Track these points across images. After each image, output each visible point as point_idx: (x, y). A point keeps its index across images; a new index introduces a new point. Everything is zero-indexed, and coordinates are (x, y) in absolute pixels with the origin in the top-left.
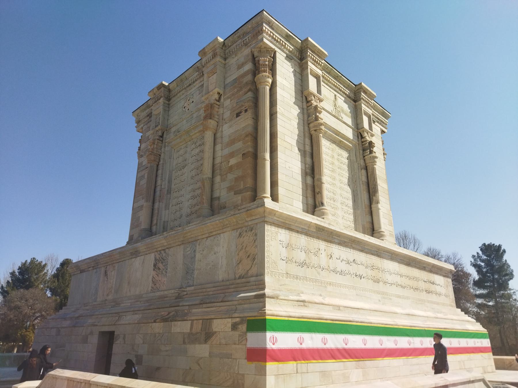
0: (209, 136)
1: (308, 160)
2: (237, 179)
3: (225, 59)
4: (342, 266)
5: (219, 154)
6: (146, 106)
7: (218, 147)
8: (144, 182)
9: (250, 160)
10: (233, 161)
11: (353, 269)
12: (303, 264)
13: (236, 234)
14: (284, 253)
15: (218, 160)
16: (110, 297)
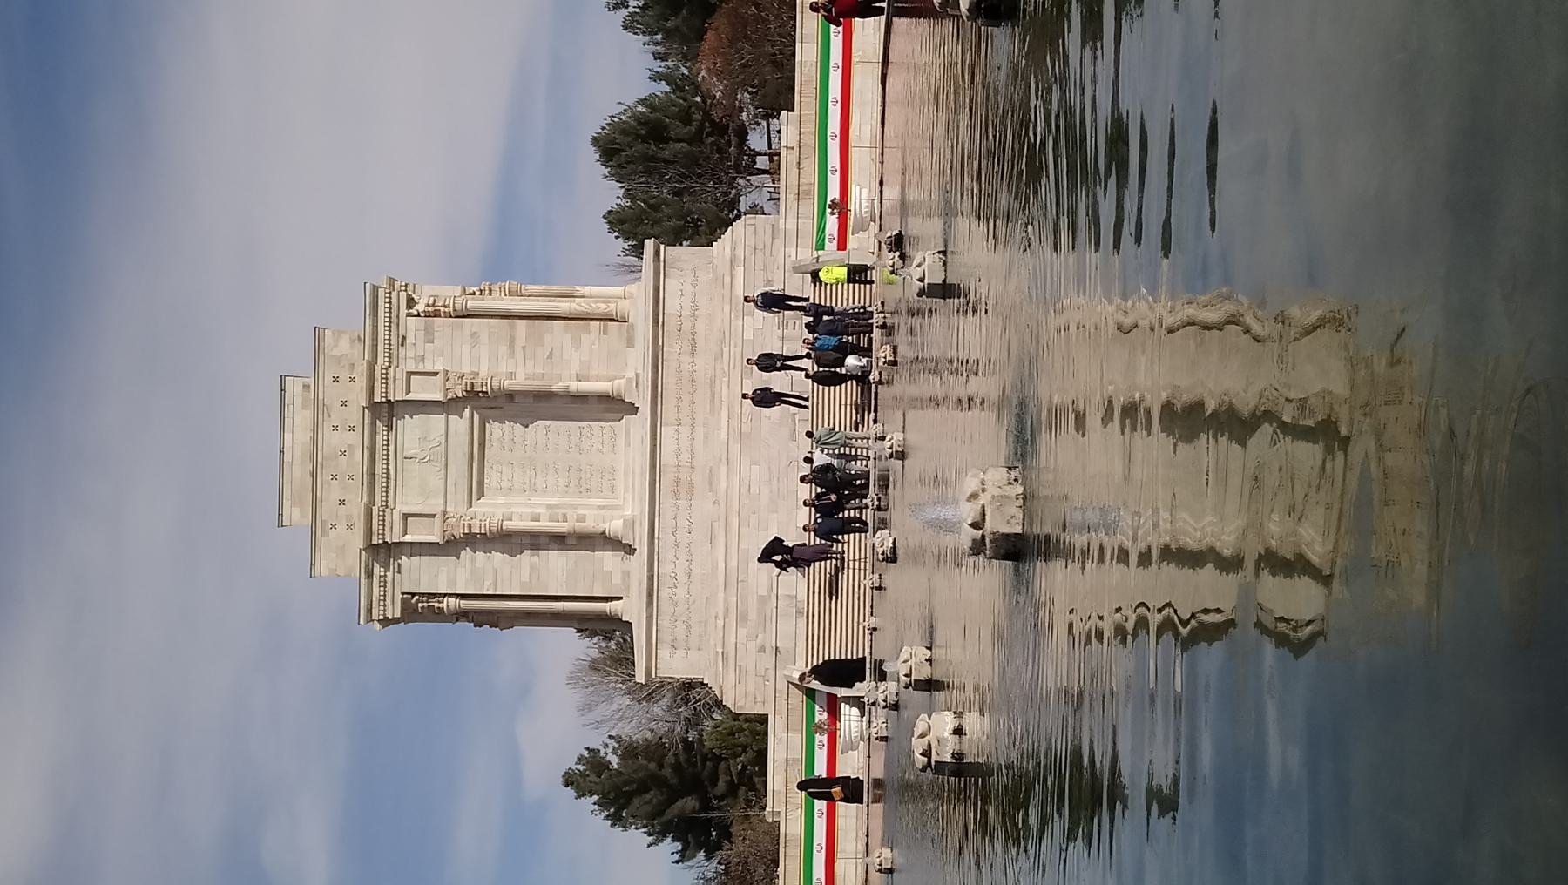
11: (683, 537)
12: (689, 627)
14: (680, 653)
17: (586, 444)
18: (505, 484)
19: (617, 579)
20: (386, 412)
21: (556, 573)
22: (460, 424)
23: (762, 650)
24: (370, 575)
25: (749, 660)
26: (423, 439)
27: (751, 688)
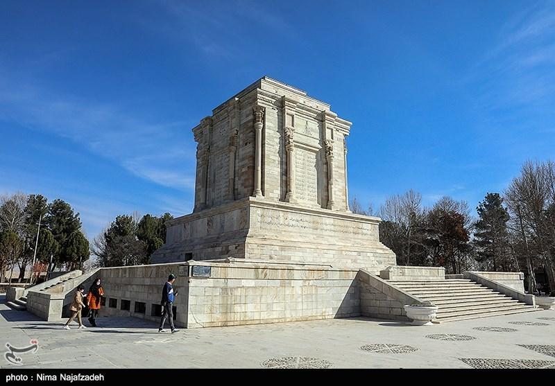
0: (232, 154)
1: (284, 166)
2: (245, 180)
3: (240, 109)
4: (292, 223)
5: (237, 165)
6: (199, 127)
7: (237, 161)
8: (200, 174)
9: (251, 170)
10: (244, 170)
11: (301, 224)
12: (269, 223)
13: (240, 211)
14: (259, 219)
15: (237, 169)
16: (188, 238)
17: (311, 189)
18: (298, 157)
19: (271, 195)
20: (321, 118)
21: (272, 170)
22: (316, 143)
23: (271, 258)
24: (273, 97)
25: (267, 250)
26: (312, 130)
27: (256, 251)
